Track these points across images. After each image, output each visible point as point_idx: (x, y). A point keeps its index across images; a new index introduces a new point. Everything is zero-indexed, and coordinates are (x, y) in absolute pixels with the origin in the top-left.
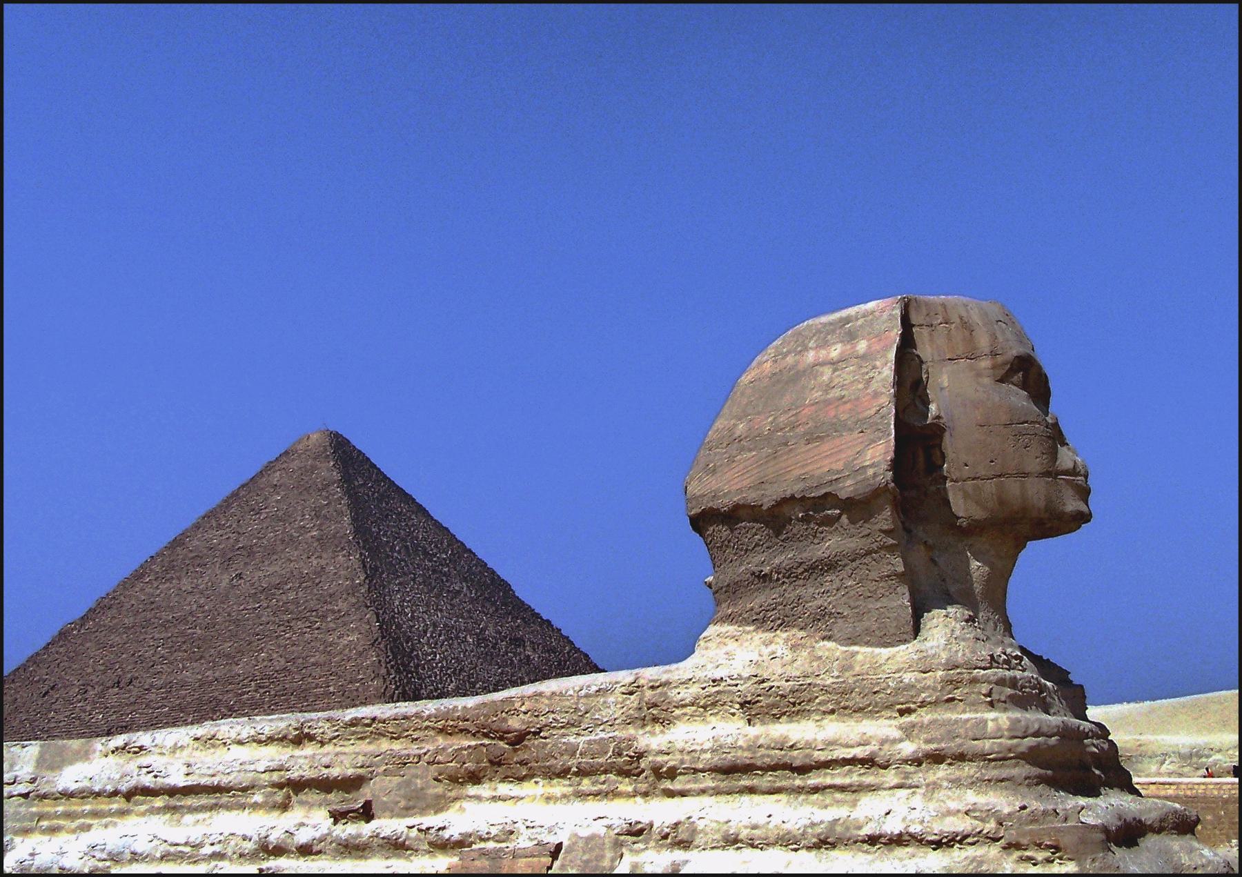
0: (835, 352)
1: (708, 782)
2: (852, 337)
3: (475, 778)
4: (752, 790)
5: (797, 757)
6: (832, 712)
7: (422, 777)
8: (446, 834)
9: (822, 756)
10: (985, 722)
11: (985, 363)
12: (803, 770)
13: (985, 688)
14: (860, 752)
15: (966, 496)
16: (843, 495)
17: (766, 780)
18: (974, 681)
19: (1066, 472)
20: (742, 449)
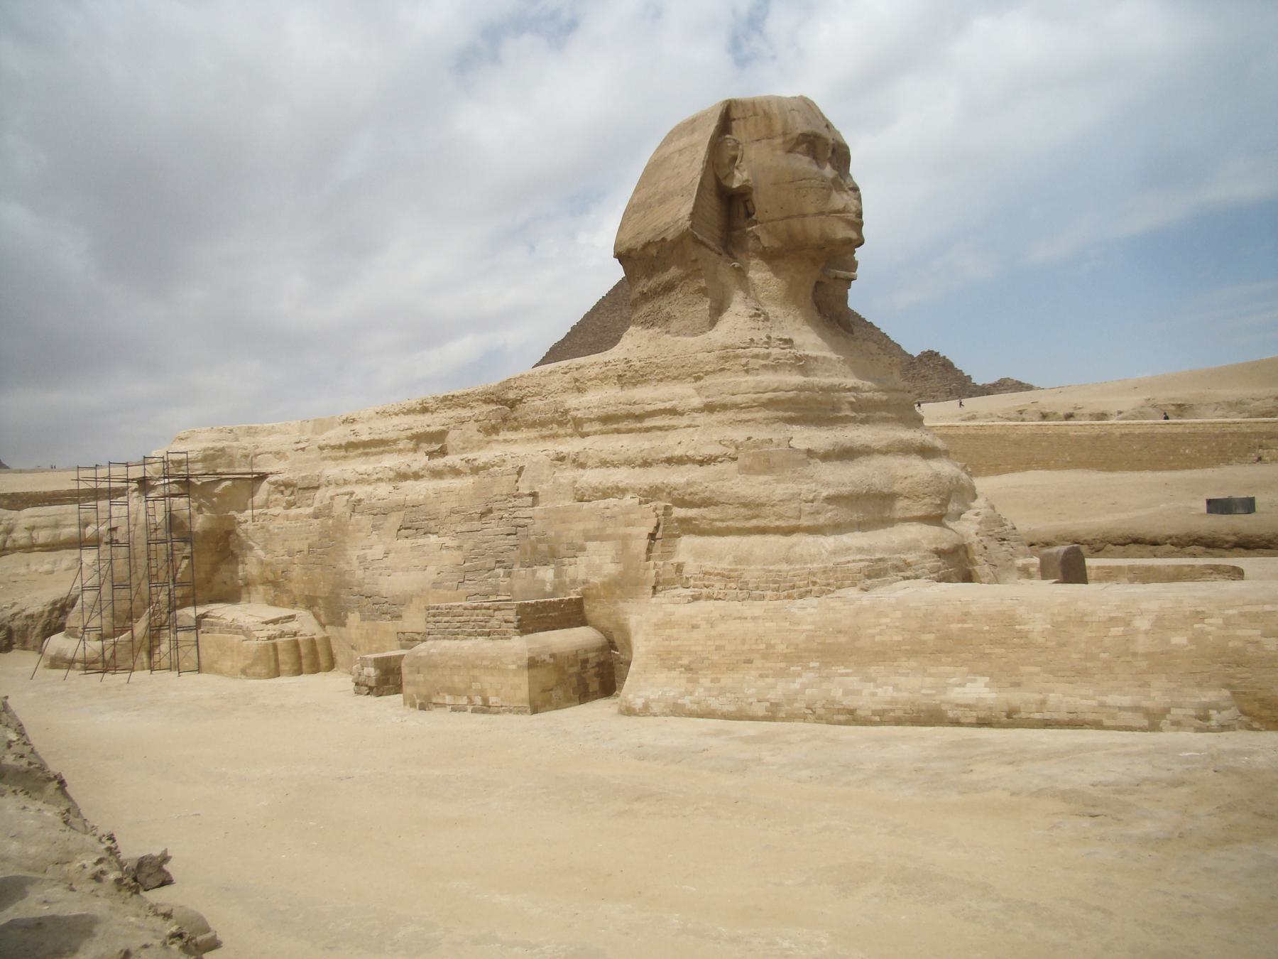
0: (684, 142)
1: (597, 426)
2: (693, 131)
3: (495, 429)
4: (618, 431)
5: (637, 410)
6: (661, 380)
7: (471, 429)
8: (476, 463)
9: (649, 408)
10: (740, 383)
11: (779, 141)
12: (639, 418)
13: (744, 361)
14: (668, 405)
15: (769, 233)
16: (669, 238)
17: (622, 425)
18: (737, 357)
19: (836, 212)
20: (635, 212)
